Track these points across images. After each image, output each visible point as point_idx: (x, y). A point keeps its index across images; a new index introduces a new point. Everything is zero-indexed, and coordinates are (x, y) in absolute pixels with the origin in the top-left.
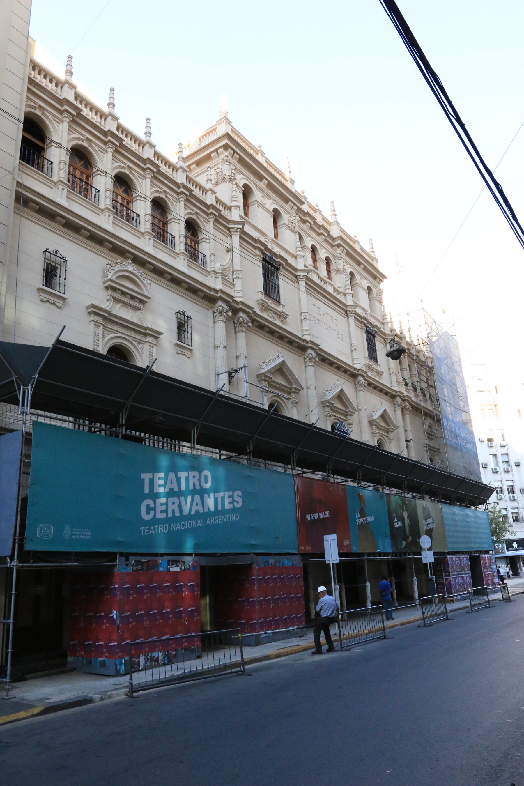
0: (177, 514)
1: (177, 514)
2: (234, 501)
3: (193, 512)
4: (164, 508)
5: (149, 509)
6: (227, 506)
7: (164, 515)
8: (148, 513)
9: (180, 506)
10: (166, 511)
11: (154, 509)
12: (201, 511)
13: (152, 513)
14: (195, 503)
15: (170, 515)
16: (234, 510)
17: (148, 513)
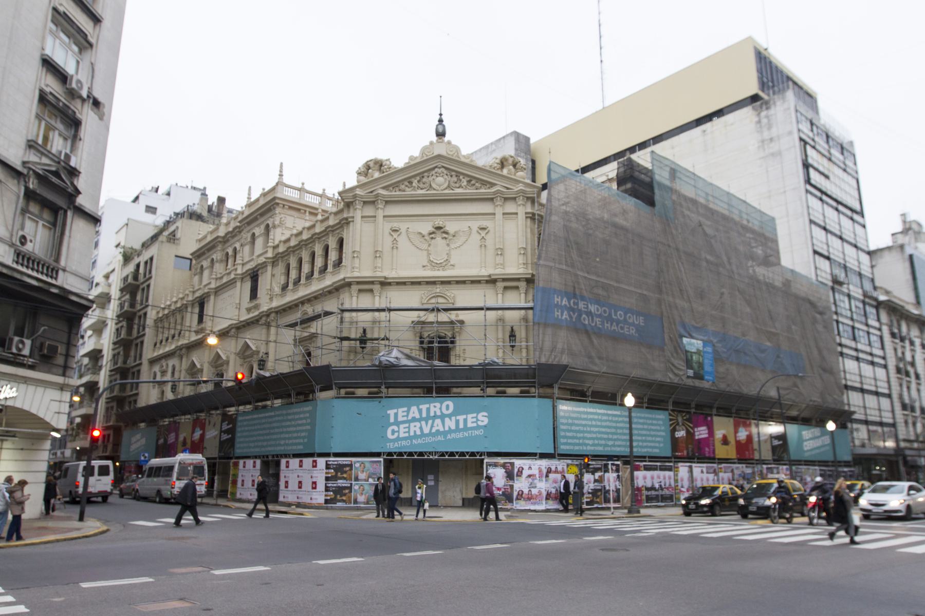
0: (418, 433)
1: (418, 433)
2: (478, 420)
3: (434, 430)
4: (407, 430)
5: (393, 432)
6: (470, 425)
7: (407, 435)
8: (393, 434)
9: (421, 428)
10: (409, 432)
11: (398, 432)
12: (442, 429)
13: (396, 434)
14: (435, 424)
15: (412, 434)
16: (478, 427)
17: (393, 434)
